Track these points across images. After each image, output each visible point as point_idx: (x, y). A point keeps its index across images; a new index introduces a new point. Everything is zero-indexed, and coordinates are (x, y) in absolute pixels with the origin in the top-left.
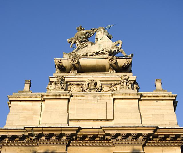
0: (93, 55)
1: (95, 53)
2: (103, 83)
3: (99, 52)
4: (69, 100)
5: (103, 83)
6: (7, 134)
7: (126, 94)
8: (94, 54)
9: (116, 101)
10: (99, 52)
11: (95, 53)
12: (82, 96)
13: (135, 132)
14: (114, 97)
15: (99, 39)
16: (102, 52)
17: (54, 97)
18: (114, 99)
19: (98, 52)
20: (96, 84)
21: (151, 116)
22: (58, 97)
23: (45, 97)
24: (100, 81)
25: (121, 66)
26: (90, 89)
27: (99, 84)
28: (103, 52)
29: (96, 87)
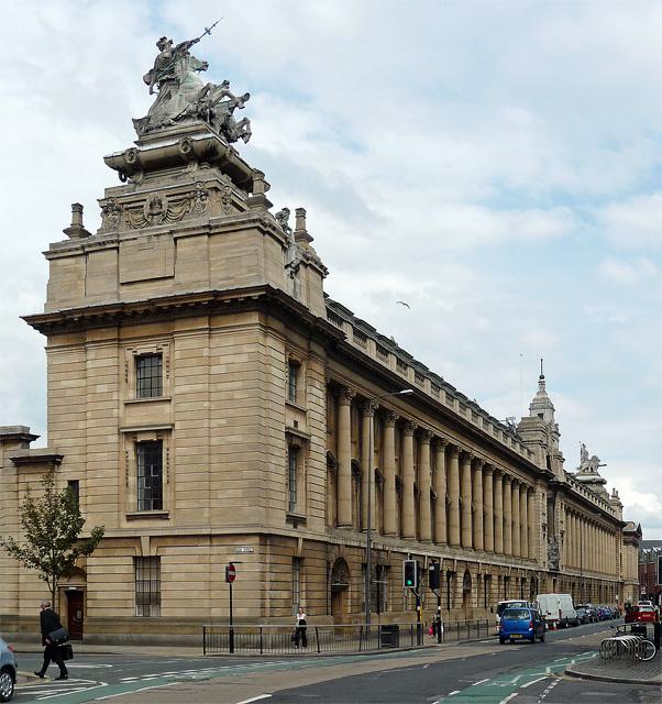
0: (170, 125)
4: (117, 248)
7: (188, 229)
14: (175, 236)
17: (99, 248)
18: (175, 239)
23: (87, 250)
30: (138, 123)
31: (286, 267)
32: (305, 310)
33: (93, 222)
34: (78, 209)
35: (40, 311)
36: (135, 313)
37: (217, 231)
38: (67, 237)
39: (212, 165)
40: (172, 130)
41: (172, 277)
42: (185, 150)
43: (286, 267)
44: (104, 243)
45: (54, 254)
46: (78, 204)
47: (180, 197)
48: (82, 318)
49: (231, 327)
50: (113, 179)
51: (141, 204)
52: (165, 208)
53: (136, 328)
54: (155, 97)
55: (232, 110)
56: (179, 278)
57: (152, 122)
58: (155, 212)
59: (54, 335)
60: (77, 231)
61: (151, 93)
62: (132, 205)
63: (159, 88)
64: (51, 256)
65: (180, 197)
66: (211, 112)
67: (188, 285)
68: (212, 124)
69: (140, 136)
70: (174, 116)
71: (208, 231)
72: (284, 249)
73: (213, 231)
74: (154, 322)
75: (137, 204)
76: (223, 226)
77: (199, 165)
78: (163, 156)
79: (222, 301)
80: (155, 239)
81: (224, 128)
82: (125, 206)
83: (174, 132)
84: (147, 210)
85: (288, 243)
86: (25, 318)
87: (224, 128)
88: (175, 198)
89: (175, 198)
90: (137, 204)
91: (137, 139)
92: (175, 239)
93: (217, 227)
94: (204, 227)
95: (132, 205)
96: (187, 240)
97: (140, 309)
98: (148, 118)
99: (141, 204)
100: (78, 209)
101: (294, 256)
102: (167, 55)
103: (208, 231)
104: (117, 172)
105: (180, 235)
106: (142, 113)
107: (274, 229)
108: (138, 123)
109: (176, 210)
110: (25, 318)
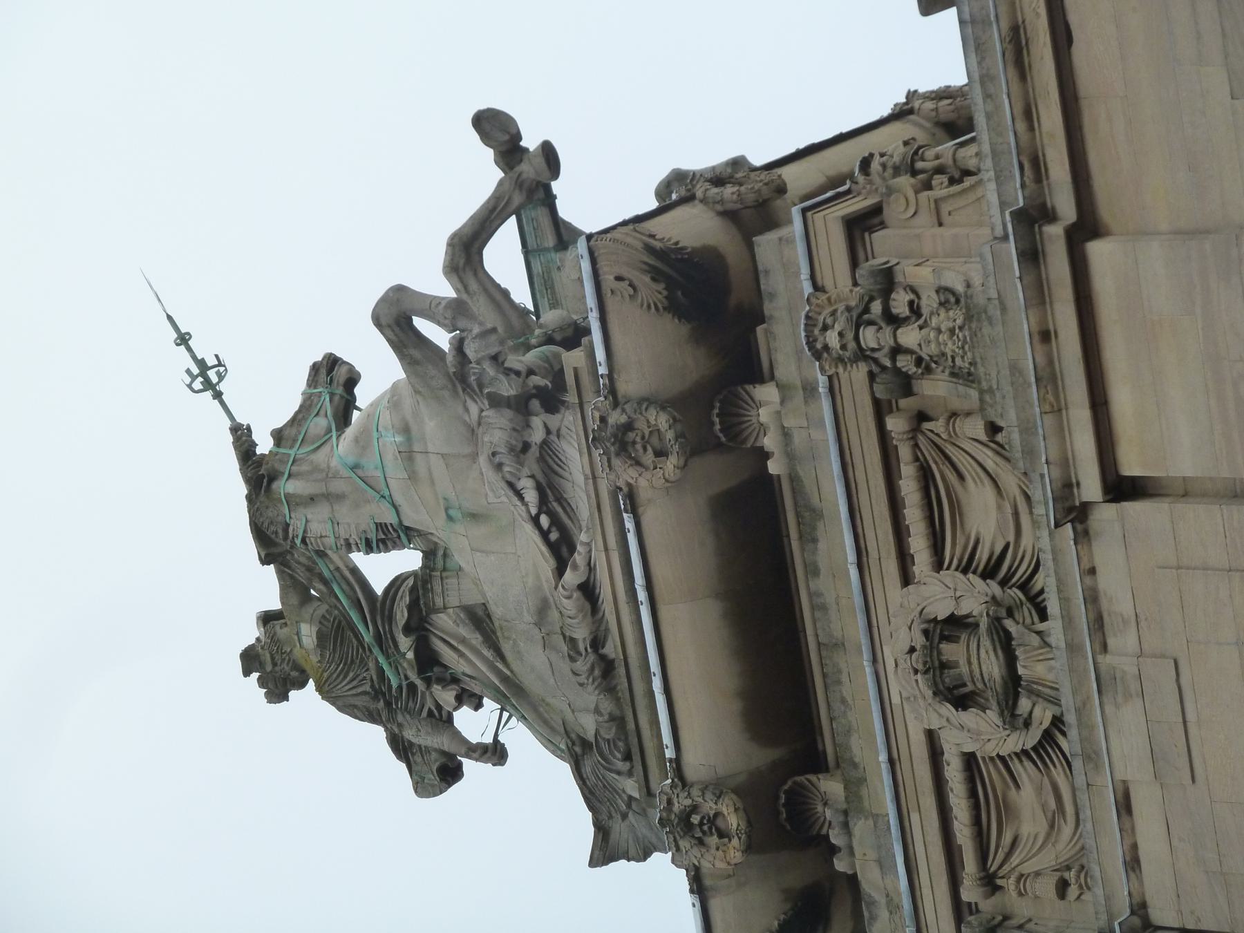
0: (588, 591)
1: (560, 571)
2: (919, 544)
3: (535, 520)
5: (919, 544)
7: (1049, 378)
8: (572, 578)
9: (1131, 466)
10: (544, 521)
11: (560, 571)
12: (1125, 806)
14: (1091, 487)
15: (390, 518)
16: (531, 496)
19: (544, 535)
20: (955, 626)
24: (906, 579)
25: (698, 337)
26: (1013, 683)
28: (539, 488)
29: (984, 623)
47: (909, 487)
57: (588, 725)
58: (992, 667)
61: (495, 753)
65: (909, 487)
70: (547, 565)
71: (1054, 233)
73: (1066, 206)
82: (969, 893)
88: (913, 515)
89: (913, 515)
94: (1032, 256)
96: (1122, 399)
103: (1054, 233)
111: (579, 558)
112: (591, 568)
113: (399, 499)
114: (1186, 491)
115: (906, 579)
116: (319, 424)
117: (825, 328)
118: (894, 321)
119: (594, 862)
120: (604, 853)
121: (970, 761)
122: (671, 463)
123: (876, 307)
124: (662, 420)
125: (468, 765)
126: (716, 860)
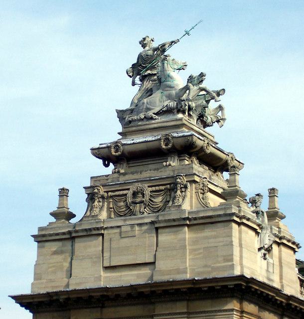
0: (152, 118)
2: (154, 189)
3: (161, 110)
4: (103, 235)
5: (154, 189)
6: (32, 301)
7: (169, 221)
9: (159, 231)
10: (161, 111)
11: (154, 114)
13: (171, 287)
14: (157, 225)
16: (164, 109)
17: (85, 233)
20: (143, 195)
21: (201, 251)
22: (89, 233)
23: (74, 235)
27: (148, 191)
28: (166, 111)
29: (143, 199)
30: (121, 114)
31: (260, 249)
32: (278, 292)
33: (78, 205)
34: (64, 193)
35: (27, 291)
36: (118, 296)
37: (195, 222)
38: (53, 220)
39: (190, 155)
40: (154, 124)
41: (153, 263)
42: (166, 145)
43: (260, 249)
44: (90, 230)
45: (41, 238)
46: (63, 189)
48: (68, 299)
49: (208, 312)
50: (99, 169)
51: (125, 192)
52: (147, 198)
53: (119, 309)
54: (137, 88)
55: (208, 102)
56: (160, 265)
58: (138, 200)
59: (39, 312)
60: (62, 215)
61: (134, 84)
62: (117, 193)
63: (141, 80)
64: (39, 239)
66: (189, 106)
67: (169, 272)
68: (190, 115)
69: (124, 128)
72: (257, 233)
74: (134, 305)
75: (121, 193)
76: (202, 218)
77: (179, 157)
78: (146, 148)
79: (201, 288)
80: (137, 228)
81: (201, 117)
83: (156, 126)
84: (130, 200)
85: (261, 228)
86: (14, 297)
87: (201, 117)
88: (157, 188)
89: (157, 188)
90: (121, 193)
91: (121, 130)
92: (157, 229)
93: (195, 219)
95: (117, 193)
97: (123, 293)
98: (131, 111)
99: (125, 192)
100: (64, 193)
101: (267, 241)
102: (150, 53)
104: (101, 161)
105: (162, 225)
106: (126, 106)
107: (248, 219)
108: (121, 114)
109: (159, 200)
110: (14, 297)
111: (157, 117)
112: (155, 119)
113: (165, 83)
114: (157, 237)
115: (149, 187)
116: (176, 67)
117: (180, 178)
118: (181, 188)
119: (116, 110)
120: (116, 110)
121: (126, 195)
122: (164, 147)
123: (182, 186)
124: (169, 146)
125: (132, 79)
126: (113, 150)
